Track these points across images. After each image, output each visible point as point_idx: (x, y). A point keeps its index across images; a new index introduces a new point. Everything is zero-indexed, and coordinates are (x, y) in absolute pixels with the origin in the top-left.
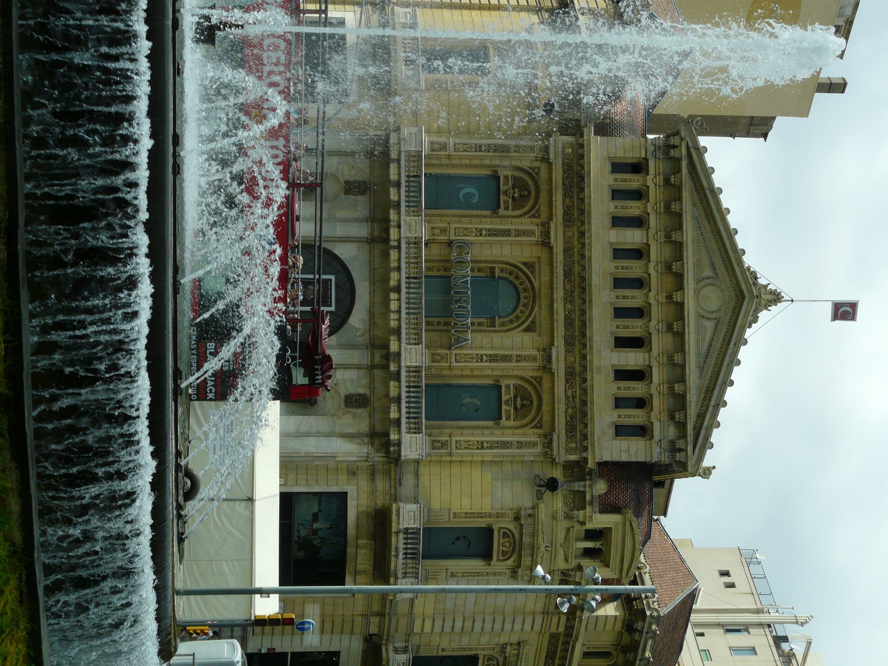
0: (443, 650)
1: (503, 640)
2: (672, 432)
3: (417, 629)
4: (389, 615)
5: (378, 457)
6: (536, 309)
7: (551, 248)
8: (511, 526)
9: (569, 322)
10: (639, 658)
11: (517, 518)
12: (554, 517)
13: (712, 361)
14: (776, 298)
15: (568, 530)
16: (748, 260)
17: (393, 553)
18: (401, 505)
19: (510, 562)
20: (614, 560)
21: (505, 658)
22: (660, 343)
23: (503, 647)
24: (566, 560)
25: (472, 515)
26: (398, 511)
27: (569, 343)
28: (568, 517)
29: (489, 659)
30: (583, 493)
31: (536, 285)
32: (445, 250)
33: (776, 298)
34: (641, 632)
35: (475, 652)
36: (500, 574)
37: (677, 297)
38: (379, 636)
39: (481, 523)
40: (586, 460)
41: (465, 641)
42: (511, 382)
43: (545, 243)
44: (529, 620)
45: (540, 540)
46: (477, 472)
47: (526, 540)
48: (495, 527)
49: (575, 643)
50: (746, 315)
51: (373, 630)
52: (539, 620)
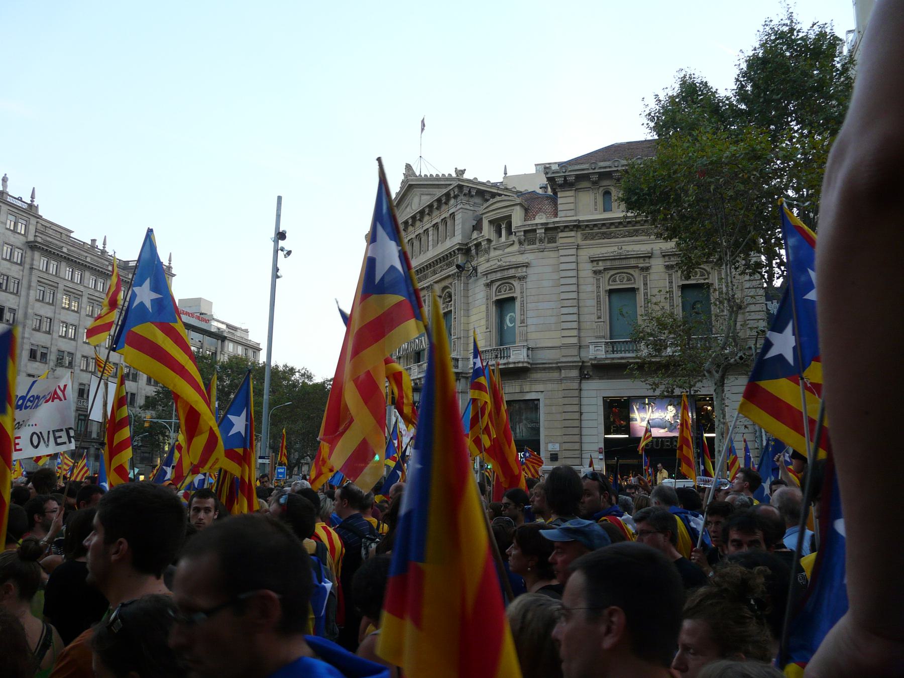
0: (599, 318)
1: (590, 274)
2: (452, 201)
3: (574, 340)
4: (557, 363)
8: (494, 288)
10: (592, 171)
11: (489, 285)
12: (488, 261)
13: (431, 190)
14: (408, 167)
15: (495, 249)
19: (515, 283)
20: (504, 212)
21: (605, 269)
22: (427, 223)
23: (595, 272)
24: (512, 244)
25: (487, 316)
27: (425, 277)
28: (487, 251)
29: (614, 281)
30: (475, 245)
32: (402, 360)
33: (408, 167)
34: (565, 177)
35: (602, 294)
36: (522, 289)
37: (410, 221)
38: (581, 369)
39: (493, 309)
40: (458, 249)
41: (589, 303)
44: (563, 259)
45: (495, 267)
46: (473, 318)
47: (499, 275)
48: (495, 299)
49: (583, 221)
50: (412, 180)
51: (575, 373)
52: (562, 252)
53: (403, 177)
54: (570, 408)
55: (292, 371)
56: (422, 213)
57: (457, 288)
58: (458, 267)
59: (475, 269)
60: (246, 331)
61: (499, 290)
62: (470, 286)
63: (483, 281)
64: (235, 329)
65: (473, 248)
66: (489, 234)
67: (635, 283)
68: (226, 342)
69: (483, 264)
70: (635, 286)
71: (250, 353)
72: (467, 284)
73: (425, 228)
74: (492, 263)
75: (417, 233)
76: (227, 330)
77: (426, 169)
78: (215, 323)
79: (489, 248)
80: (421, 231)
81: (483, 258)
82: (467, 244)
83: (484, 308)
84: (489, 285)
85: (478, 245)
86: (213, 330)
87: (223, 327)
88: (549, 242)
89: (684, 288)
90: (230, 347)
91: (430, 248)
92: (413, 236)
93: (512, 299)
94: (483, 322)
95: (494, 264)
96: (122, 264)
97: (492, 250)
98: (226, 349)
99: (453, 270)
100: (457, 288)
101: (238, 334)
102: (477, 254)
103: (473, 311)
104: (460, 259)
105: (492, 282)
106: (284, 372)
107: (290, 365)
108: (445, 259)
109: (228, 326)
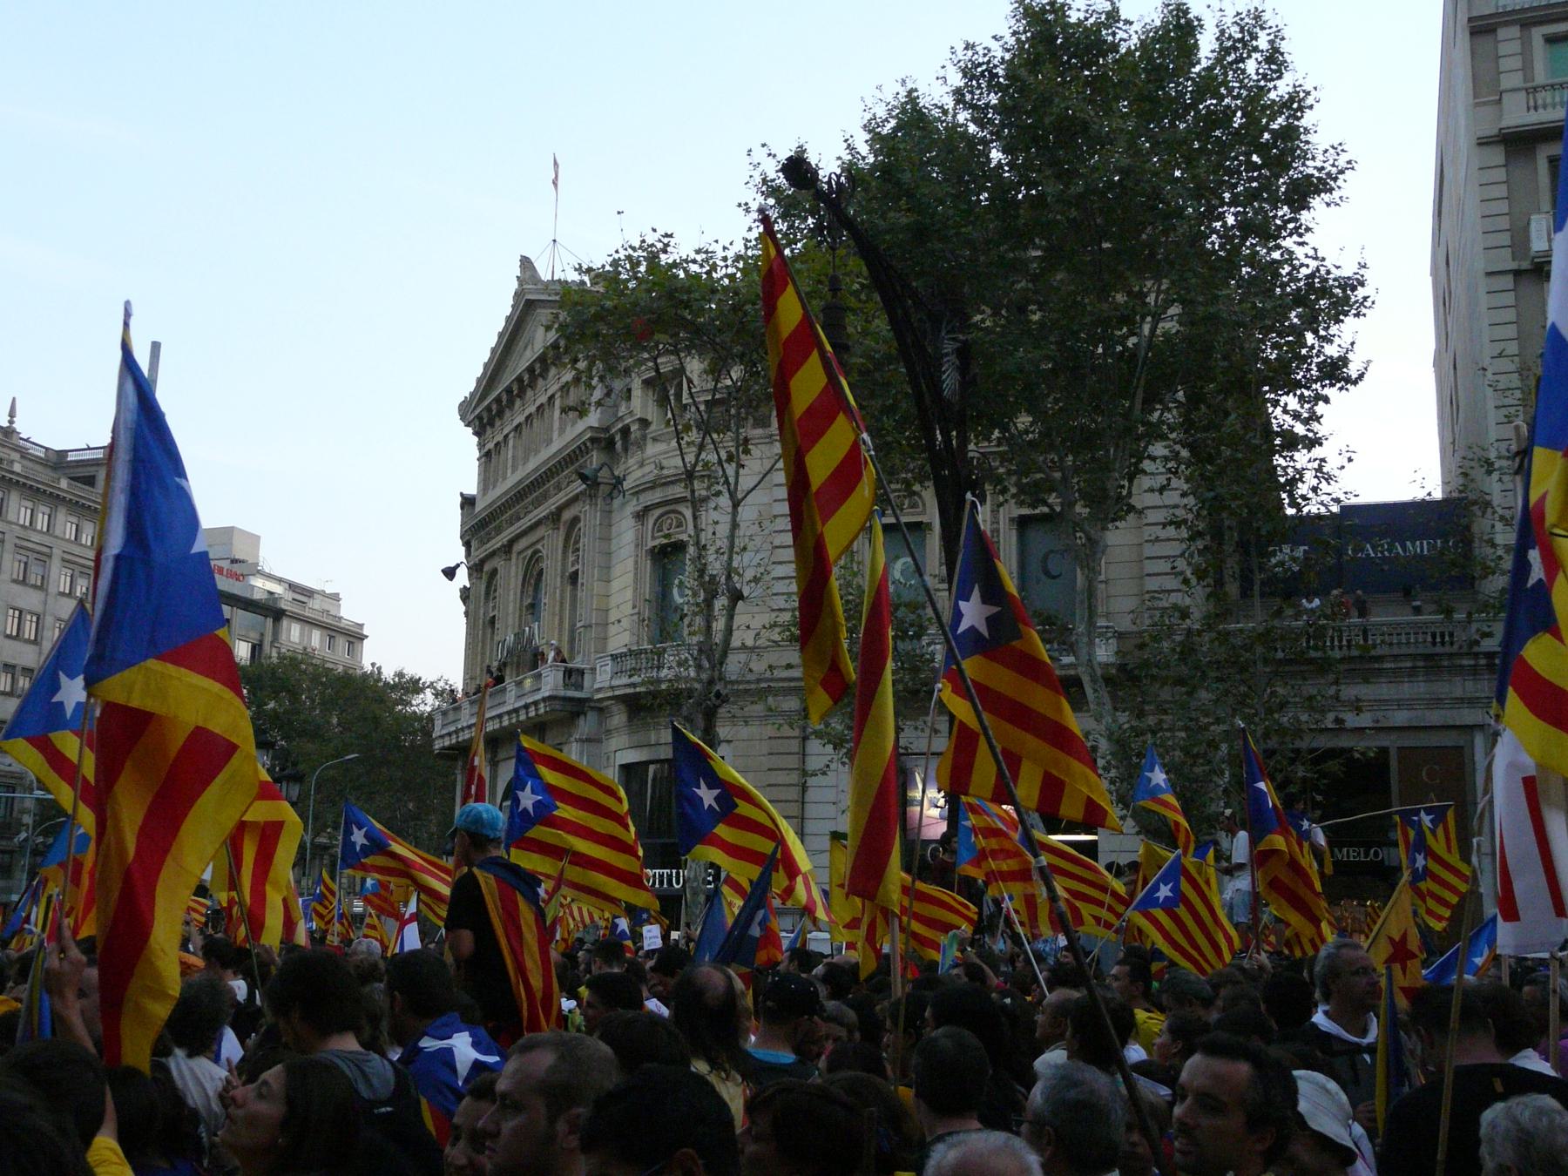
5: (586, 726)
6: (539, 546)
7: (512, 542)
9: (537, 503)
11: (641, 516)
12: (642, 465)
14: (526, 263)
15: (655, 439)
16: (508, 311)
17: (631, 691)
18: (597, 686)
25: (635, 582)
26: (599, 690)
31: (530, 552)
33: (526, 263)
37: (526, 377)
40: (592, 440)
42: (571, 559)
43: (508, 548)
47: (656, 496)
48: (651, 544)
53: (515, 285)
54: (781, 778)
55: (415, 686)
56: (542, 359)
57: (590, 515)
58: (583, 478)
59: (619, 481)
60: (335, 598)
61: (658, 526)
62: (616, 517)
63: (633, 506)
64: (309, 593)
65: (618, 438)
66: (644, 406)
67: (923, 512)
68: (285, 622)
69: (635, 470)
70: (925, 519)
71: (341, 642)
72: (608, 513)
73: (550, 393)
74: (647, 469)
75: (538, 403)
76: (289, 596)
77: (559, 267)
78: (258, 582)
79: (644, 437)
80: (543, 399)
81: (631, 461)
82: (607, 429)
83: (630, 563)
84: (641, 516)
85: (625, 431)
86: (257, 596)
87: (278, 589)
88: (755, 426)
89: (1023, 523)
90: (293, 634)
91: (555, 435)
92: (532, 409)
93: (680, 547)
94: (629, 594)
95: (649, 472)
96: (53, 458)
97: (649, 442)
98: (283, 637)
99: (578, 486)
100: (590, 515)
101: (316, 604)
102: (626, 449)
103: (617, 570)
104: (595, 459)
105: (647, 509)
106: (394, 687)
107: (411, 671)
108: (572, 457)
109: (292, 587)
